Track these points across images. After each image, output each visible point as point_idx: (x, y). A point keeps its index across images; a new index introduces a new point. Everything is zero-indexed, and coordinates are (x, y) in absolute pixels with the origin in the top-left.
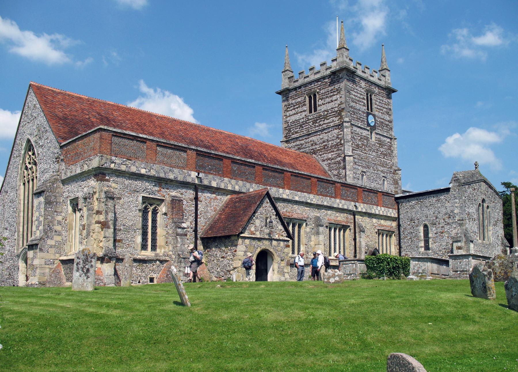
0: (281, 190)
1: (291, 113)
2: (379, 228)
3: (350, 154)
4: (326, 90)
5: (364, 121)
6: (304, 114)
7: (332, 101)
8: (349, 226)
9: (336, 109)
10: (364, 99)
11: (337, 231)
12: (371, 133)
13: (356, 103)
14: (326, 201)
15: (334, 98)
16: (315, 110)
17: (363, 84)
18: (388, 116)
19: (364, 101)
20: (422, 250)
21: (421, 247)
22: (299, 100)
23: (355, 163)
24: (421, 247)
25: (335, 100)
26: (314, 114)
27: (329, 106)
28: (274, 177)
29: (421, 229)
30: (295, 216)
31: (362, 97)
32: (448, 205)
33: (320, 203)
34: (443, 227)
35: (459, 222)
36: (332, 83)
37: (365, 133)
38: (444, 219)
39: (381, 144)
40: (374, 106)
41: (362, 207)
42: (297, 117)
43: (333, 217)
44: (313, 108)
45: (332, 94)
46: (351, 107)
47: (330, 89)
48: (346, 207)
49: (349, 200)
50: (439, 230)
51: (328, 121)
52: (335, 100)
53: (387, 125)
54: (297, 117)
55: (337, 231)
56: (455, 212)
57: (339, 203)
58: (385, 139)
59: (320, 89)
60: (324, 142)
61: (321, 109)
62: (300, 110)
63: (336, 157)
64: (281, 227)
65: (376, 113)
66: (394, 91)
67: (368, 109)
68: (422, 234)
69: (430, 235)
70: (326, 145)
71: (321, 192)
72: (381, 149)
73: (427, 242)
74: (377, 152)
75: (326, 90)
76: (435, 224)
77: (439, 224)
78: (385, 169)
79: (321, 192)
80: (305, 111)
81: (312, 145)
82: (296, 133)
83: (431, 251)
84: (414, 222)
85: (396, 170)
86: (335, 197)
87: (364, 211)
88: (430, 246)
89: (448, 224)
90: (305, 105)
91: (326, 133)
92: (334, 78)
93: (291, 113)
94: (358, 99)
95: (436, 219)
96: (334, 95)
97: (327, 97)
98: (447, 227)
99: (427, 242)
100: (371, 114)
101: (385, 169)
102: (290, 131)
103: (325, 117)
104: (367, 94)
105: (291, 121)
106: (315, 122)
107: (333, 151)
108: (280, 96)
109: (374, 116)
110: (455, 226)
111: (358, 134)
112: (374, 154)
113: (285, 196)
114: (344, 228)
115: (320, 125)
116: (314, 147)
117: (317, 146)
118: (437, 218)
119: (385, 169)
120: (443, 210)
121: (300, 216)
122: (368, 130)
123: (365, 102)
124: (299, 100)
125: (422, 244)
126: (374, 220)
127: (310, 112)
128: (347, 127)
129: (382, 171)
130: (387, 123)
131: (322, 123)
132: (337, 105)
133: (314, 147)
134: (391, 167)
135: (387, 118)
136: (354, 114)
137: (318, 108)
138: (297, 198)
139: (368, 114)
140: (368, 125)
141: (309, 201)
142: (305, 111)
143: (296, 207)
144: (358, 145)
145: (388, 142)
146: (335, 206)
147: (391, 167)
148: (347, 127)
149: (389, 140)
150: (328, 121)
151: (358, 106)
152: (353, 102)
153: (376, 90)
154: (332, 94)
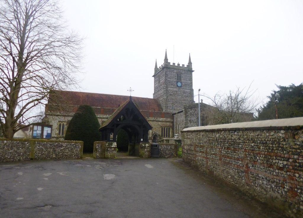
6: (158, 84)
10: (175, 77)
17: (175, 71)
37: (175, 89)
39: (184, 93)
46: (168, 81)
53: (189, 85)
61: (161, 82)
66: (193, 71)
67: (178, 79)
108: (153, 77)
109: (181, 82)
112: (180, 97)
123: (176, 78)
126: (160, 123)
130: (189, 84)
135: (189, 82)
136: (170, 83)
139: (177, 82)
140: (177, 86)
151: (172, 80)
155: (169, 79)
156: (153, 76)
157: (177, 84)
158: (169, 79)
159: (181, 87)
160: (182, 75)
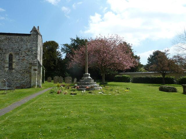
20: (7, 69)
21: (7, 67)
24: (7, 67)
29: (7, 56)
32: (29, 44)
34: (24, 56)
35: (35, 55)
38: (25, 52)
50: (21, 58)
56: (33, 49)
68: (8, 59)
69: (14, 60)
73: (11, 65)
76: (19, 54)
77: (21, 54)
83: (14, 70)
84: (2, 51)
88: (14, 67)
89: (28, 55)
95: (20, 51)
98: (26, 57)
99: (11, 65)
110: (32, 57)
118: (20, 50)
120: (25, 47)
125: (7, 65)
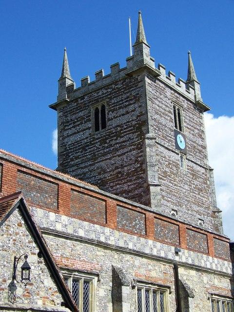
0: (52, 216)
1: (70, 132)
2: (213, 292)
3: (156, 182)
4: (119, 99)
5: (171, 141)
6: (87, 132)
7: (127, 113)
8: (169, 288)
9: (134, 123)
10: (170, 112)
11: (151, 295)
12: (181, 157)
13: (160, 115)
14: (133, 242)
15: (131, 108)
16: (104, 126)
17: (169, 92)
18: (200, 140)
19: (170, 115)
22: (81, 114)
23: (163, 197)
25: (133, 111)
26: (102, 133)
27: (123, 120)
28: (40, 190)
30: (78, 266)
31: (167, 109)
33: (121, 244)
36: (128, 87)
37: (175, 157)
39: (194, 175)
40: (184, 124)
41: (186, 256)
42: (78, 137)
43: (143, 271)
44: (101, 121)
45: (127, 103)
46: (155, 120)
47: (125, 96)
48: (163, 255)
49: (167, 243)
51: (122, 140)
52: (133, 111)
53: (200, 152)
54: (78, 137)
55: (151, 295)
57: (151, 246)
58: (199, 168)
59: (111, 99)
60: (117, 168)
61: (112, 124)
62: (82, 127)
63: (135, 189)
64: (49, 282)
65: (186, 133)
70: (120, 172)
71: (123, 226)
72: (196, 182)
74: (190, 186)
75: (119, 99)
78: (201, 209)
79: (123, 226)
80: (89, 128)
81: (100, 174)
82: (77, 158)
85: (214, 212)
86: (146, 236)
87: (190, 262)
90: (89, 120)
91: (119, 156)
92: (130, 82)
93: (70, 132)
94: (163, 111)
96: (131, 104)
97: (120, 108)
100: (179, 133)
101: (201, 209)
102: (67, 155)
103: (118, 135)
104: (174, 107)
105: (69, 143)
106: (103, 141)
107: (131, 181)
109: (184, 136)
111: (165, 157)
112: (186, 187)
113: (59, 228)
114: (162, 289)
115: (111, 146)
116: (102, 176)
117: (106, 175)
119: (202, 209)
121: (88, 267)
122: (178, 154)
123: (173, 116)
124: (81, 114)
126: (205, 278)
127: (97, 129)
128: (150, 146)
129: (197, 212)
130: (200, 148)
131: (113, 142)
132: (134, 118)
133: (102, 176)
134: (208, 208)
137: (108, 123)
138: (81, 233)
139: (176, 133)
140: (178, 147)
141: (102, 239)
142: (89, 128)
143: (80, 246)
144: (165, 172)
145: (203, 173)
146: (147, 251)
147: (208, 208)
148: (150, 146)
149: (203, 170)
150: (122, 140)
152: (157, 113)
153: (185, 104)
154: (127, 103)
155: (156, 116)
156: (53, 107)
157: (176, 143)
158: (156, 116)
159: (183, 152)
160: (182, 113)
